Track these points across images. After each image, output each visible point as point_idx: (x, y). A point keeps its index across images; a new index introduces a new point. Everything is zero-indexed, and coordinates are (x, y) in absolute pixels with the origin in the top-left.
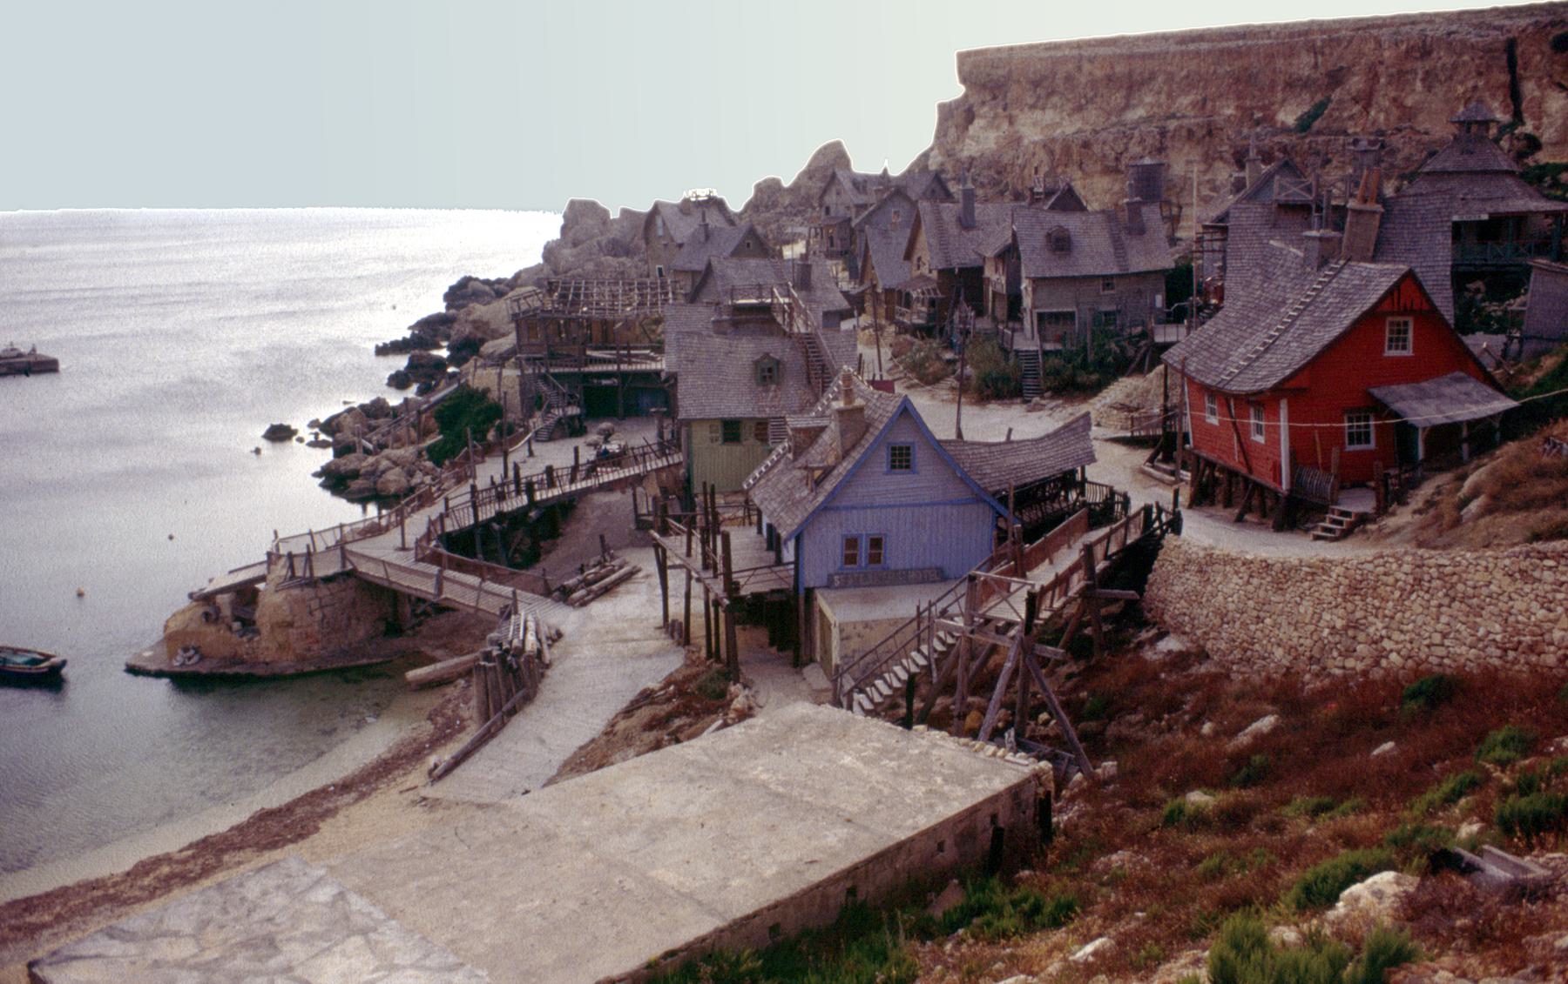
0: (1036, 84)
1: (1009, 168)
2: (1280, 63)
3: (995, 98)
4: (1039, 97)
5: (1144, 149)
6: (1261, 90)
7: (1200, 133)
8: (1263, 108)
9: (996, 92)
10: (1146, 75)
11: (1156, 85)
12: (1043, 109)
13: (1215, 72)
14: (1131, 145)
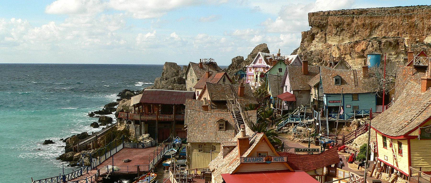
0: (337, 26)
1: (325, 56)
2: (425, 21)
3: (322, 31)
4: (338, 31)
5: (373, 49)
6: (419, 30)
7: (394, 43)
8: (420, 37)
9: (323, 29)
10: (377, 24)
11: (380, 28)
12: (339, 36)
13: (402, 24)
14: (368, 47)
